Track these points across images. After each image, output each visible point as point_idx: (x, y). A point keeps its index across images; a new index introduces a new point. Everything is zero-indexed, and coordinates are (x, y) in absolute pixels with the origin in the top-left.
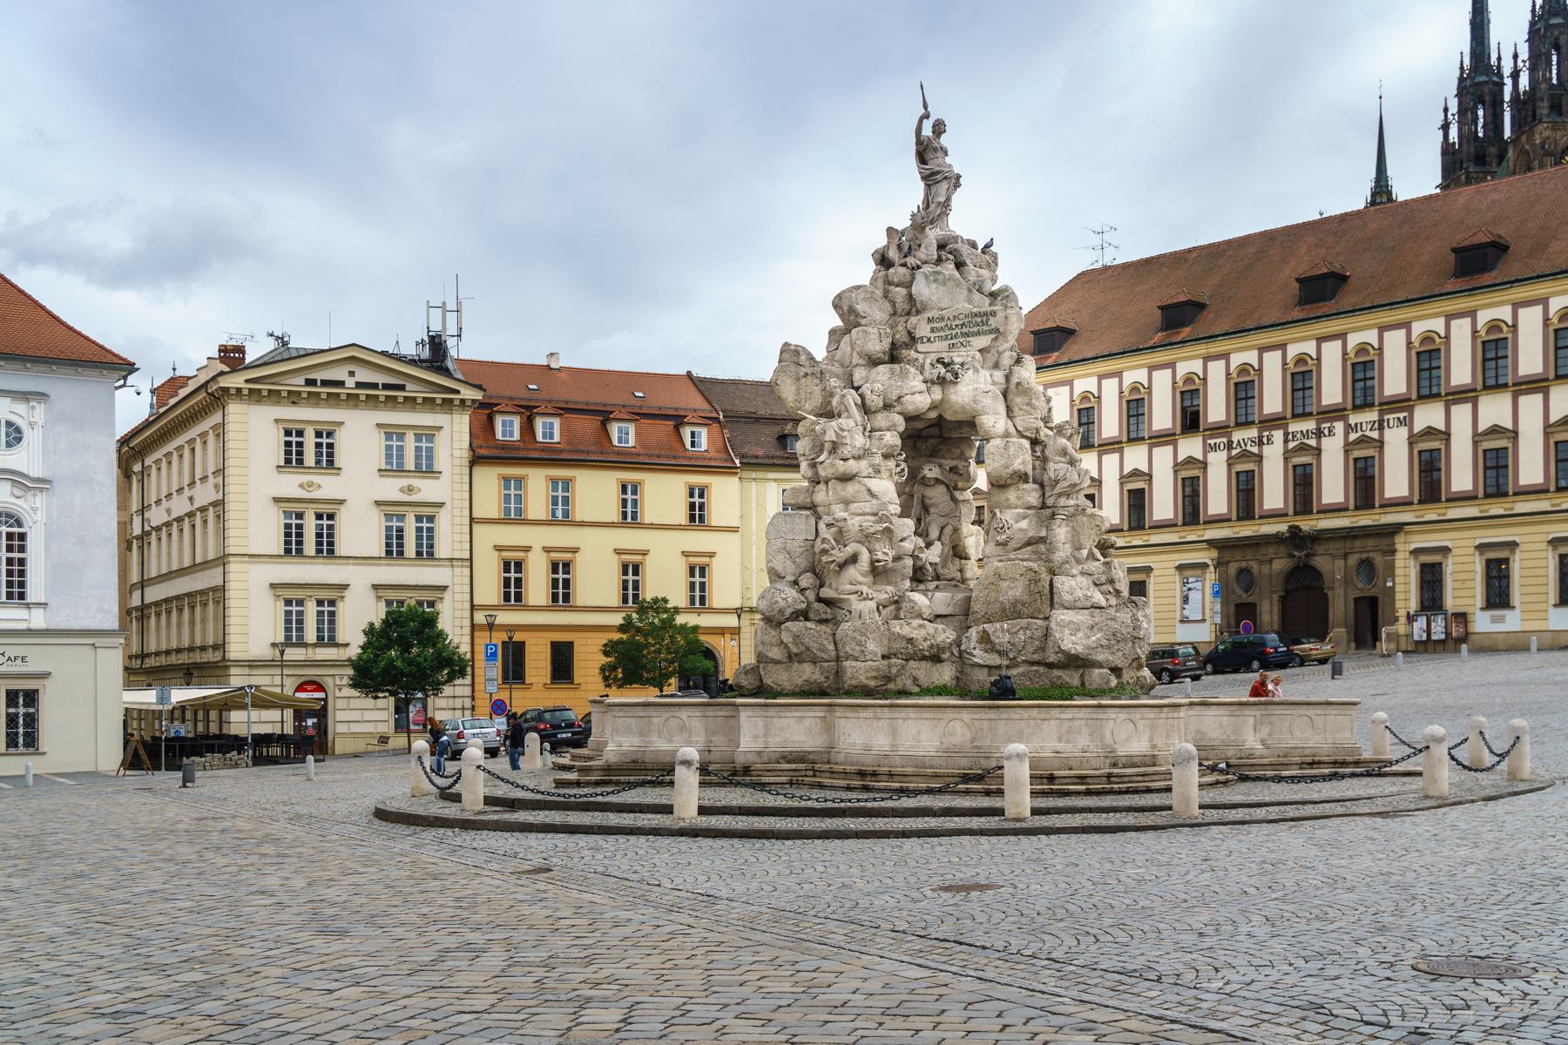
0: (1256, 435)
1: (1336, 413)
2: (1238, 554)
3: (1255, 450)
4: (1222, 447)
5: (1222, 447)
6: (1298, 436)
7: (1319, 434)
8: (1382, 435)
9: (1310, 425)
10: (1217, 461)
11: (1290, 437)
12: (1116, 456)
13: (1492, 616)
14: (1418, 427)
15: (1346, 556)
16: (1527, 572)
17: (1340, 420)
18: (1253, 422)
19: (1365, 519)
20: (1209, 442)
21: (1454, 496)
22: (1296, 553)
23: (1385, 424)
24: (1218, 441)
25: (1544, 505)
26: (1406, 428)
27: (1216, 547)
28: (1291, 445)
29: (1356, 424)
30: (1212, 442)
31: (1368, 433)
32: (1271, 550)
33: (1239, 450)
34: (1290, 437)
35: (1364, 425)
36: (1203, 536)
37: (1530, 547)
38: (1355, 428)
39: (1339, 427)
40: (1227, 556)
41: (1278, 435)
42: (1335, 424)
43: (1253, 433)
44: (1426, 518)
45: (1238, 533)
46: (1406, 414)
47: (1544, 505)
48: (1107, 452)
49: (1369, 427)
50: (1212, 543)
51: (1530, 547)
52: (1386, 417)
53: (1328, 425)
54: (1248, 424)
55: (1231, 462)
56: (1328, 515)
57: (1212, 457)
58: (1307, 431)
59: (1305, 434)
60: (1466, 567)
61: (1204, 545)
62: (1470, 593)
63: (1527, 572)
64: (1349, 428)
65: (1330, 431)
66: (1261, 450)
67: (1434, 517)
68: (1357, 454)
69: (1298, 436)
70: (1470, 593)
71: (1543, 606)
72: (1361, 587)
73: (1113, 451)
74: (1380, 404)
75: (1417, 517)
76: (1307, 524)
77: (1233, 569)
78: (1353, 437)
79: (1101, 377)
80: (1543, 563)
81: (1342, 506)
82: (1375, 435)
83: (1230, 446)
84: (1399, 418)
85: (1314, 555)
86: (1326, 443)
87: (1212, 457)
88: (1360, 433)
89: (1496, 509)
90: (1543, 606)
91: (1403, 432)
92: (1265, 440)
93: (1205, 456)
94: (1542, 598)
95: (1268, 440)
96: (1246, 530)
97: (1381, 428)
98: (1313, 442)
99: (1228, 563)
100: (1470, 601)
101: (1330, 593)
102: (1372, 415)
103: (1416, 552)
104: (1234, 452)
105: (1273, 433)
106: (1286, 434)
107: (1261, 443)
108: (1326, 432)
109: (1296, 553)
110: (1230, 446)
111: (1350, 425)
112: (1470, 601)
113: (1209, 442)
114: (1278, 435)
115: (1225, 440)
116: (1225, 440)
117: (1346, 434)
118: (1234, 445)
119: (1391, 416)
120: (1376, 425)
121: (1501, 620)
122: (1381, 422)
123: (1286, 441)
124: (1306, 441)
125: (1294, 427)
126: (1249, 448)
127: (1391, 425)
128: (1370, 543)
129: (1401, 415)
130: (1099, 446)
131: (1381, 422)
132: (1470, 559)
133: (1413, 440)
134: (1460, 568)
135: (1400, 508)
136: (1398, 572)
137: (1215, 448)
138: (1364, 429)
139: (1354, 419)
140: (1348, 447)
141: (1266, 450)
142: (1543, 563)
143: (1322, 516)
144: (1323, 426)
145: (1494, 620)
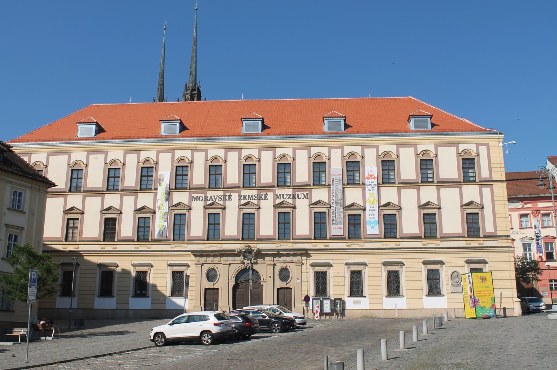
0: (222, 195)
1: (268, 187)
2: (209, 259)
3: (221, 202)
4: (201, 199)
5: (201, 199)
6: (247, 197)
7: (259, 198)
8: (294, 202)
9: (254, 192)
10: (198, 208)
11: (242, 197)
12: (133, 198)
13: (354, 301)
14: (314, 200)
15: (274, 265)
16: (372, 279)
17: (271, 192)
18: (220, 188)
19: (284, 246)
20: (193, 195)
21: (368, 236)
22: (245, 261)
23: (296, 196)
24: (199, 195)
25: (379, 245)
26: (308, 199)
27: (196, 256)
28: (243, 202)
29: (280, 195)
30: (195, 195)
31: (287, 200)
32: (230, 259)
33: (211, 202)
34: (242, 197)
35: (285, 196)
36: (186, 248)
37: (373, 265)
38: (279, 197)
39: (270, 195)
40: (203, 259)
41: (235, 196)
42: (268, 193)
43: (220, 193)
44: (318, 247)
45: (209, 247)
46: (307, 192)
47: (379, 245)
48: (127, 194)
49: (287, 197)
50: (192, 251)
51: (373, 265)
52: (297, 193)
53: (265, 193)
54: (217, 188)
55: (206, 207)
56: (263, 242)
57: (194, 204)
58: (252, 195)
59: (252, 197)
60: (340, 274)
61: (190, 253)
62: (342, 288)
63: (372, 279)
64: (276, 197)
65: (265, 197)
66: (224, 203)
67: (323, 247)
68: (281, 210)
69: (247, 197)
70: (342, 288)
71: (380, 296)
72: (279, 284)
73: (131, 194)
74: (293, 186)
75: (313, 246)
76: (256, 246)
77: (205, 268)
78: (278, 201)
79: (126, 152)
80: (379, 274)
81: (272, 237)
82: (291, 201)
83: (206, 199)
84: (303, 194)
85: (256, 263)
86: (263, 203)
87: (194, 204)
88: (282, 200)
89: (355, 245)
90: (380, 296)
91: (306, 202)
92: (227, 198)
93: (190, 203)
94: (379, 292)
95: (229, 198)
96: (213, 246)
97: (294, 198)
98: (255, 202)
99: (202, 265)
100: (342, 292)
101: (264, 285)
102: (290, 191)
103: (313, 265)
104: (208, 203)
105: (232, 194)
106: (240, 196)
107: (224, 199)
108: (264, 198)
109: (245, 261)
110: (206, 199)
111: (277, 195)
112: (342, 292)
113: (193, 195)
114: (235, 196)
115: (203, 195)
116: (203, 195)
117: (275, 199)
118: (208, 199)
119: (300, 193)
120: (291, 197)
121: (360, 303)
122: (294, 195)
123: (240, 200)
124: (251, 201)
125: (244, 192)
126: (217, 201)
127: (300, 197)
128: (289, 259)
129: (305, 193)
130: (121, 191)
131: (294, 195)
132: (342, 270)
133: (312, 205)
134: (336, 274)
135: (304, 241)
136: (304, 275)
137: (196, 199)
138: (285, 198)
139: (279, 192)
140: (276, 206)
141: (228, 204)
142: (379, 274)
143: (260, 242)
144: (261, 194)
145: (355, 303)
